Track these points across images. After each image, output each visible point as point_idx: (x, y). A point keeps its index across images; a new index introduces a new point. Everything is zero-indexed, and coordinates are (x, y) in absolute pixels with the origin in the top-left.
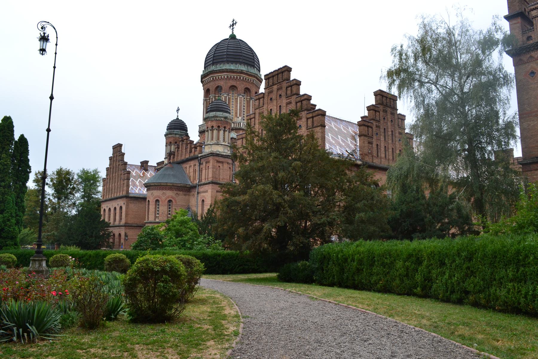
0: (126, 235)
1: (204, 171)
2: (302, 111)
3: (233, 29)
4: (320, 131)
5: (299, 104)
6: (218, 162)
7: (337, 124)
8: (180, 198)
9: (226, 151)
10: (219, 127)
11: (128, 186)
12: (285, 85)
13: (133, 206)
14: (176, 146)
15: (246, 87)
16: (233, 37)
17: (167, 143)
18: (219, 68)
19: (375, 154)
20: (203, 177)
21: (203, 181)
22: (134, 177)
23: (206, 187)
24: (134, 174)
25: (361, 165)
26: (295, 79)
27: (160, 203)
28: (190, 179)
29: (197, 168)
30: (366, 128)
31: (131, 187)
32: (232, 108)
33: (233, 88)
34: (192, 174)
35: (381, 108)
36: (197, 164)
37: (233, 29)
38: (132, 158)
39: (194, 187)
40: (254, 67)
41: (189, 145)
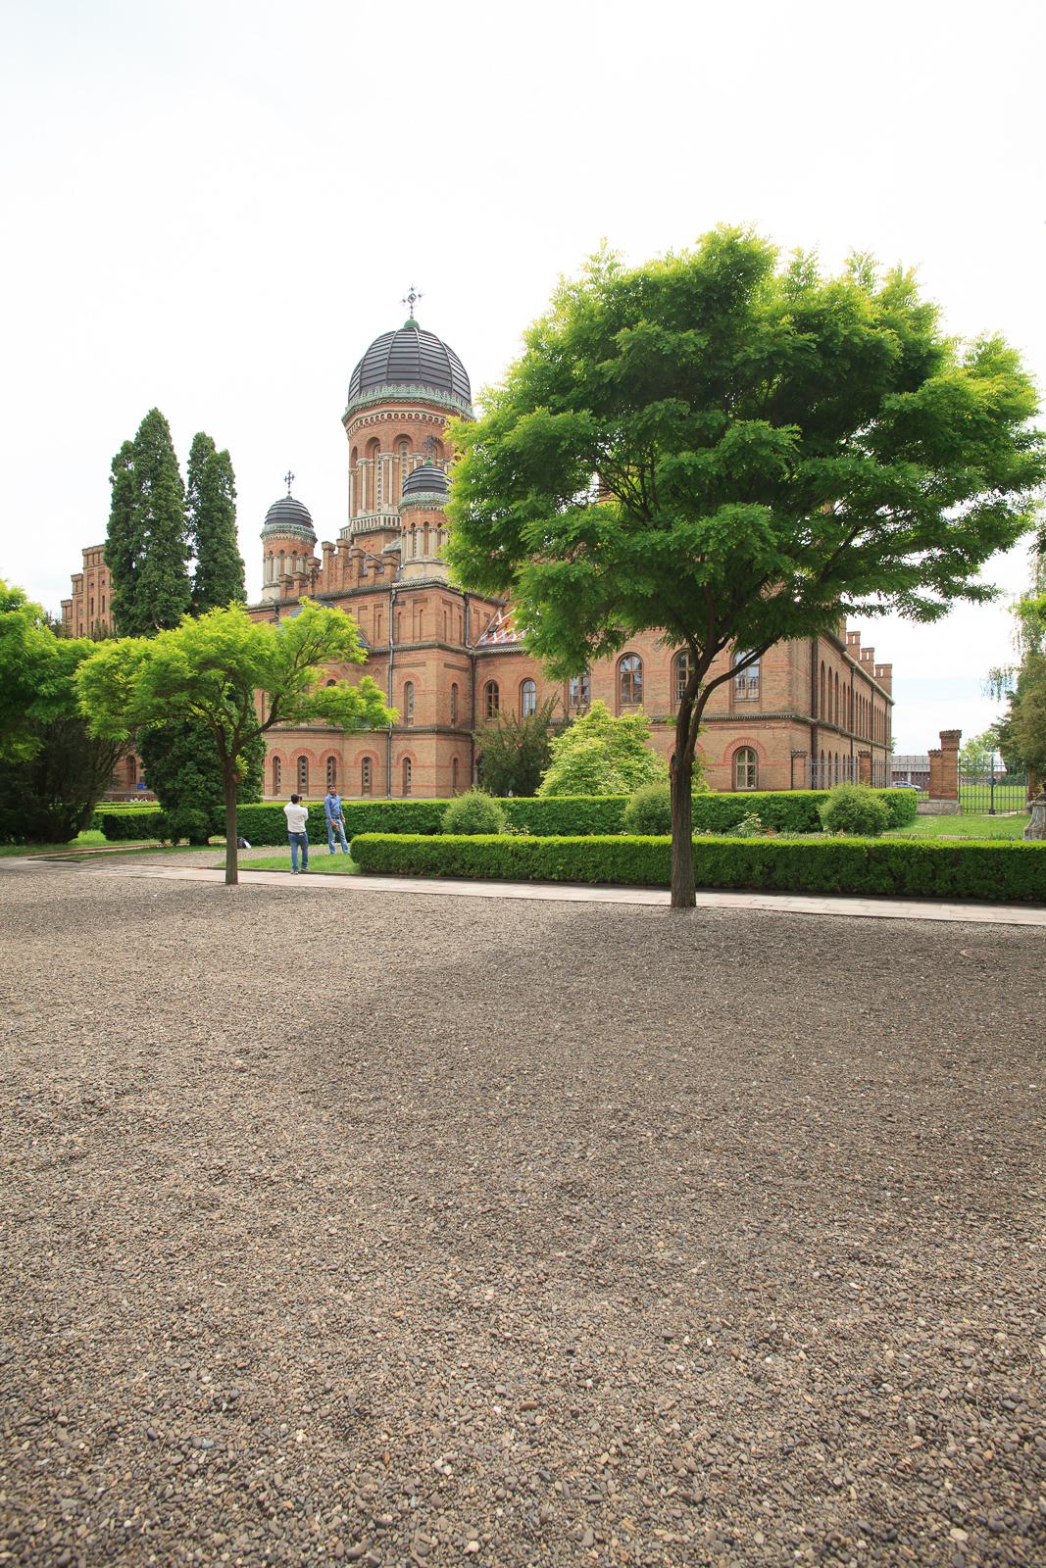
6: (445, 602)
21: (408, 643)
23: (421, 655)
29: (386, 612)
36: (387, 604)
39: (384, 654)
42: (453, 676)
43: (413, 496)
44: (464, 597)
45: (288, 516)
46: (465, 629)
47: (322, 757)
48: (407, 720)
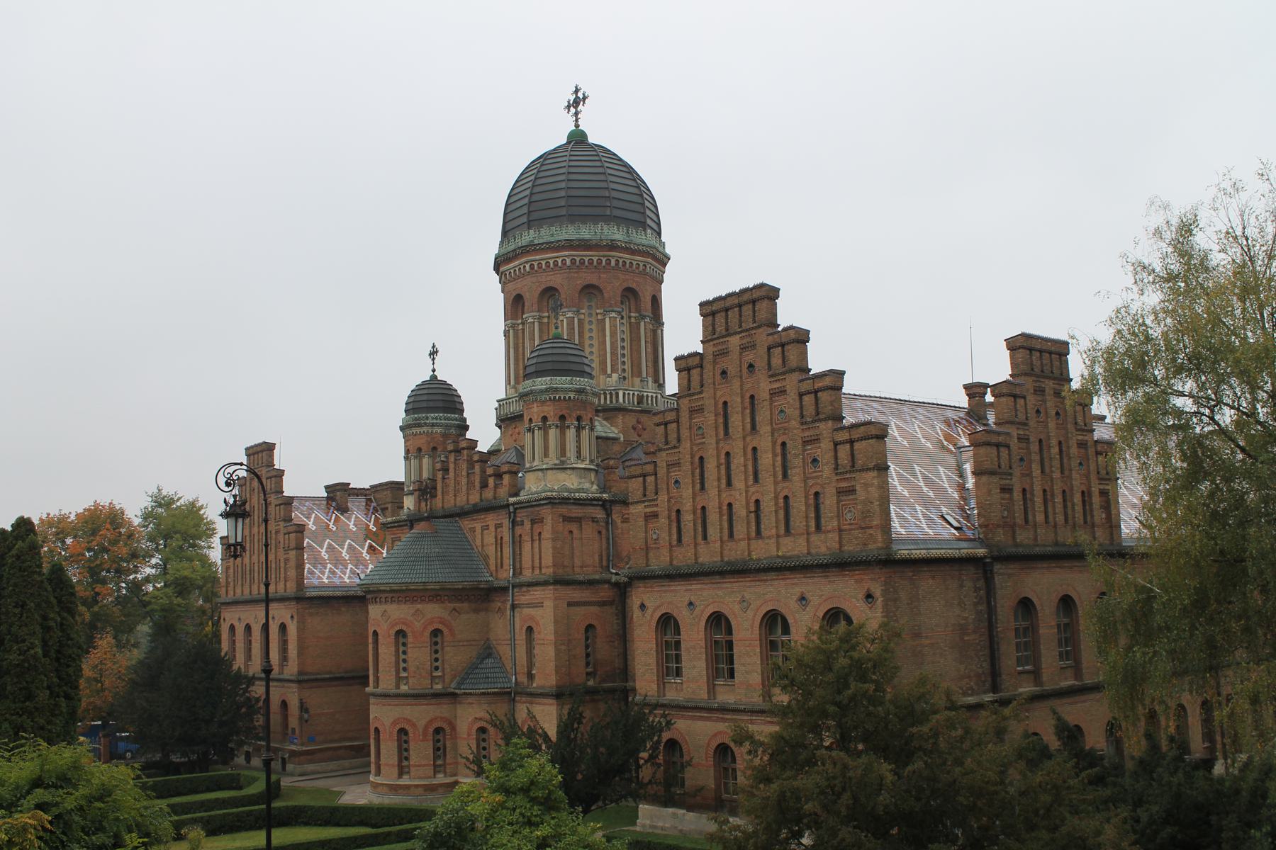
0: (303, 707)
1: (527, 547)
2: (820, 420)
3: (576, 114)
4: (875, 482)
5: (808, 399)
6: (567, 519)
7: (905, 421)
8: (464, 623)
9: (587, 485)
10: (562, 418)
11: (300, 566)
12: (762, 338)
13: (321, 623)
14: (438, 466)
15: (625, 285)
16: (578, 138)
17: (407, 452)
18: (547, 238)
19: (1019, 520)
20: (527, 562)
21: (527, 575)
22: (314, 537)
23: (538, 593)
24: (311, 525)
25: (985, 557)
26: (792, 328)
27: (410, 639)
28: (488, 564)
30: (994, 450)
31: (307, 566)
32: (591, 353)
33: (590, 290)
34: (491, 551)
35: (1029, 383)
36: (506, 523)
37: (576, 114)
38: (303, 479)
39: (504, 590)
40: (644, 225)
41: (477, 468)
42: (582, 616)
43: (528, 385)
44: (603, 506)
45: (424, 405)
46: (608, 548)
47: (426, 727)
48: (531, 677)
